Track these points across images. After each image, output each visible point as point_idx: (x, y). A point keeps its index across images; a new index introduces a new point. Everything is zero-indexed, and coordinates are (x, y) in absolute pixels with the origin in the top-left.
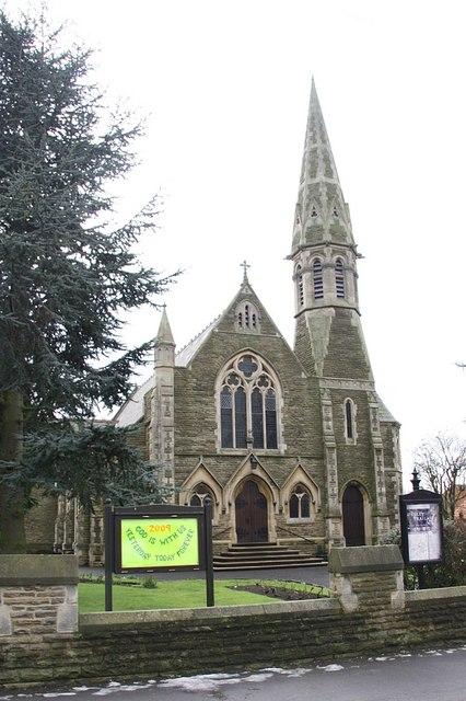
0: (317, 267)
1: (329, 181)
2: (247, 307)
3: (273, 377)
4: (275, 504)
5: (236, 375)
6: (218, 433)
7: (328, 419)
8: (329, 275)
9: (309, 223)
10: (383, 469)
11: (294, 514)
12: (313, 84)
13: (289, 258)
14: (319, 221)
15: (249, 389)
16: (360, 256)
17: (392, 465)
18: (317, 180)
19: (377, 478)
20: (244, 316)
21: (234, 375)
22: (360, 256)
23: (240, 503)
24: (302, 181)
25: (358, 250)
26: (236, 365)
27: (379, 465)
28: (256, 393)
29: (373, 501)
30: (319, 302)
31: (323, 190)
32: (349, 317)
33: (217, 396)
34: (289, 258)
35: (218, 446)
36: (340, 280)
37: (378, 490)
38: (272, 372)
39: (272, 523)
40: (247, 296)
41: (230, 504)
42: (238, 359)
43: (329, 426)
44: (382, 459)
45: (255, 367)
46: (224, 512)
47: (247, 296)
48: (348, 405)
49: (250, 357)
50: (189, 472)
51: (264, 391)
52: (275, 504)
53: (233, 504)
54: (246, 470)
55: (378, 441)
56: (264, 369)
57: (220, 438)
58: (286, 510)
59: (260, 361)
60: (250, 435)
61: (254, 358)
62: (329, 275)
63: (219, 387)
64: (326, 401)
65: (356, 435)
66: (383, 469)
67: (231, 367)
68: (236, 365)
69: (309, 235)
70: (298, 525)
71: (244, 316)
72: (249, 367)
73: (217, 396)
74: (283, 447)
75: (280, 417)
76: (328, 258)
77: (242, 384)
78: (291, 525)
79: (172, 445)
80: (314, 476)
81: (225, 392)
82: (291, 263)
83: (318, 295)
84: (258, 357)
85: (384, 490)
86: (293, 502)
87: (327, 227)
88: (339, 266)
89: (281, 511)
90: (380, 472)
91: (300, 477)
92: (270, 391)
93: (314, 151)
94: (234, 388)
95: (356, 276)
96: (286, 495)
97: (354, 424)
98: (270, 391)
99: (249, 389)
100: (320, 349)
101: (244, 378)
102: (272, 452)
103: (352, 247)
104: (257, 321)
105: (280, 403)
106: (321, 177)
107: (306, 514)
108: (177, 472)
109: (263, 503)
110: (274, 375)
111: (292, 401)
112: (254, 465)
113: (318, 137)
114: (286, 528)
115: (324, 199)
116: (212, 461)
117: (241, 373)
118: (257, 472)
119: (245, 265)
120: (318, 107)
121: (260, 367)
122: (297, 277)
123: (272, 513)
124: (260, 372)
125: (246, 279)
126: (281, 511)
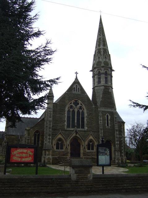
0: (99, 74)
1: (104, 47)
2: (76, 86)
3: (84, 107)
4: (83, 146)
5: (72, 106)
6: (66, 123)
7: (101, 120)
8: (103, 76)
9: (97, 60)
10: (118, 136)
11: (89, 149)
12: (101, 16)
13: (91, 71)
14: (101, 60)
15: (76, 110)
16: (113, 71)
17: (121, 135)
18: (100, 47)
19: (116, 139)
20: (75, 88)
21: (71, 106)
22: (113, 71)
23: (71, 144)
24: (96, 48)
25: (113, 69)
26: (72, 103)
27: (117, 135)
28: (78, 112)
29: (115, 146)
30: (100, 85)
31: (102, 51)
32: (109, 89)
33: (66, 112)
34: (91, 71)
35: (66, 127)
36: (106, 78)
37: (116, 143)
38: (84, 106)
39: (82, 151)
40: (76, 82)
41: (68, 145)
42: (73, 101)
43: (101, 122)
44: (118, 133)
45: (78, 104)
46: (66, 147)
47: (76, 82)
48: (107, 116)
49: (77, 101)
50: (56, 135)
51: (81, 111)
52: (83, 146)
53: (70, 145)
54: (74, 135)
55: (116, 127)
56: (81, 104)
57: (66, 125)
58: (86, 147)
59: (80, 102)
60: (76, 124)
61: (78, 101)
62: (103, 76)
63: (67, 109)
64: (100, 114)
65: (110, 125)
66: (118, 136)
67: (71, 103)
68: (72, 103)
69: (97, 65)
70: (90, 152)
71: (75, 88)
72: (76, 103)
73: (66, 112)
74: (86, 128)
75: (85, 119)
76: (103, 71)
77: (74, 109)
78: (88, 152)
79: (51, 126)
80: (96, 137)
81: (69, 111)
82: (92, 72)
83: (99, 82)
84: (79, 101)
85: (118, 143)
86: (89, 145)
87: (103, 62)
88: (106, 74)
89: (85, 148)
90: (117, 137)
91: (91, 137)
92: (83, 111)
93: (100, 39)
94: (71, 110)
95: (112, 77)
96: (86, 143)
97: (109, 122)
98: (83, 111)
99: (76, 110)
100: (99, 100)
101: (75, 107)
102: (82, 129)
103: (111, 68)
104: (80, 90)
105: (86, 115)
106: (101, 47)
107: (93, 149)
108: (52, 134)
109: (79, 145)
110: (84, 106)
111: (89, 115)
112: (77, 133)
113: (101, 34)
114: (86, 153)
115: (102, 53)
116: (64, 132)
117: (74, 105)
118: (78, 135)
119: (76, 73)
120: (102, 25)
121: (80, 104)
122: (93, 77)
123: (82, 148)
124: (80, 105)
125: (76, 77)
126: (85, 148)
